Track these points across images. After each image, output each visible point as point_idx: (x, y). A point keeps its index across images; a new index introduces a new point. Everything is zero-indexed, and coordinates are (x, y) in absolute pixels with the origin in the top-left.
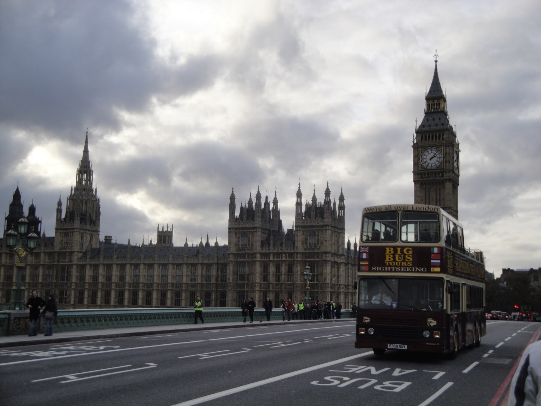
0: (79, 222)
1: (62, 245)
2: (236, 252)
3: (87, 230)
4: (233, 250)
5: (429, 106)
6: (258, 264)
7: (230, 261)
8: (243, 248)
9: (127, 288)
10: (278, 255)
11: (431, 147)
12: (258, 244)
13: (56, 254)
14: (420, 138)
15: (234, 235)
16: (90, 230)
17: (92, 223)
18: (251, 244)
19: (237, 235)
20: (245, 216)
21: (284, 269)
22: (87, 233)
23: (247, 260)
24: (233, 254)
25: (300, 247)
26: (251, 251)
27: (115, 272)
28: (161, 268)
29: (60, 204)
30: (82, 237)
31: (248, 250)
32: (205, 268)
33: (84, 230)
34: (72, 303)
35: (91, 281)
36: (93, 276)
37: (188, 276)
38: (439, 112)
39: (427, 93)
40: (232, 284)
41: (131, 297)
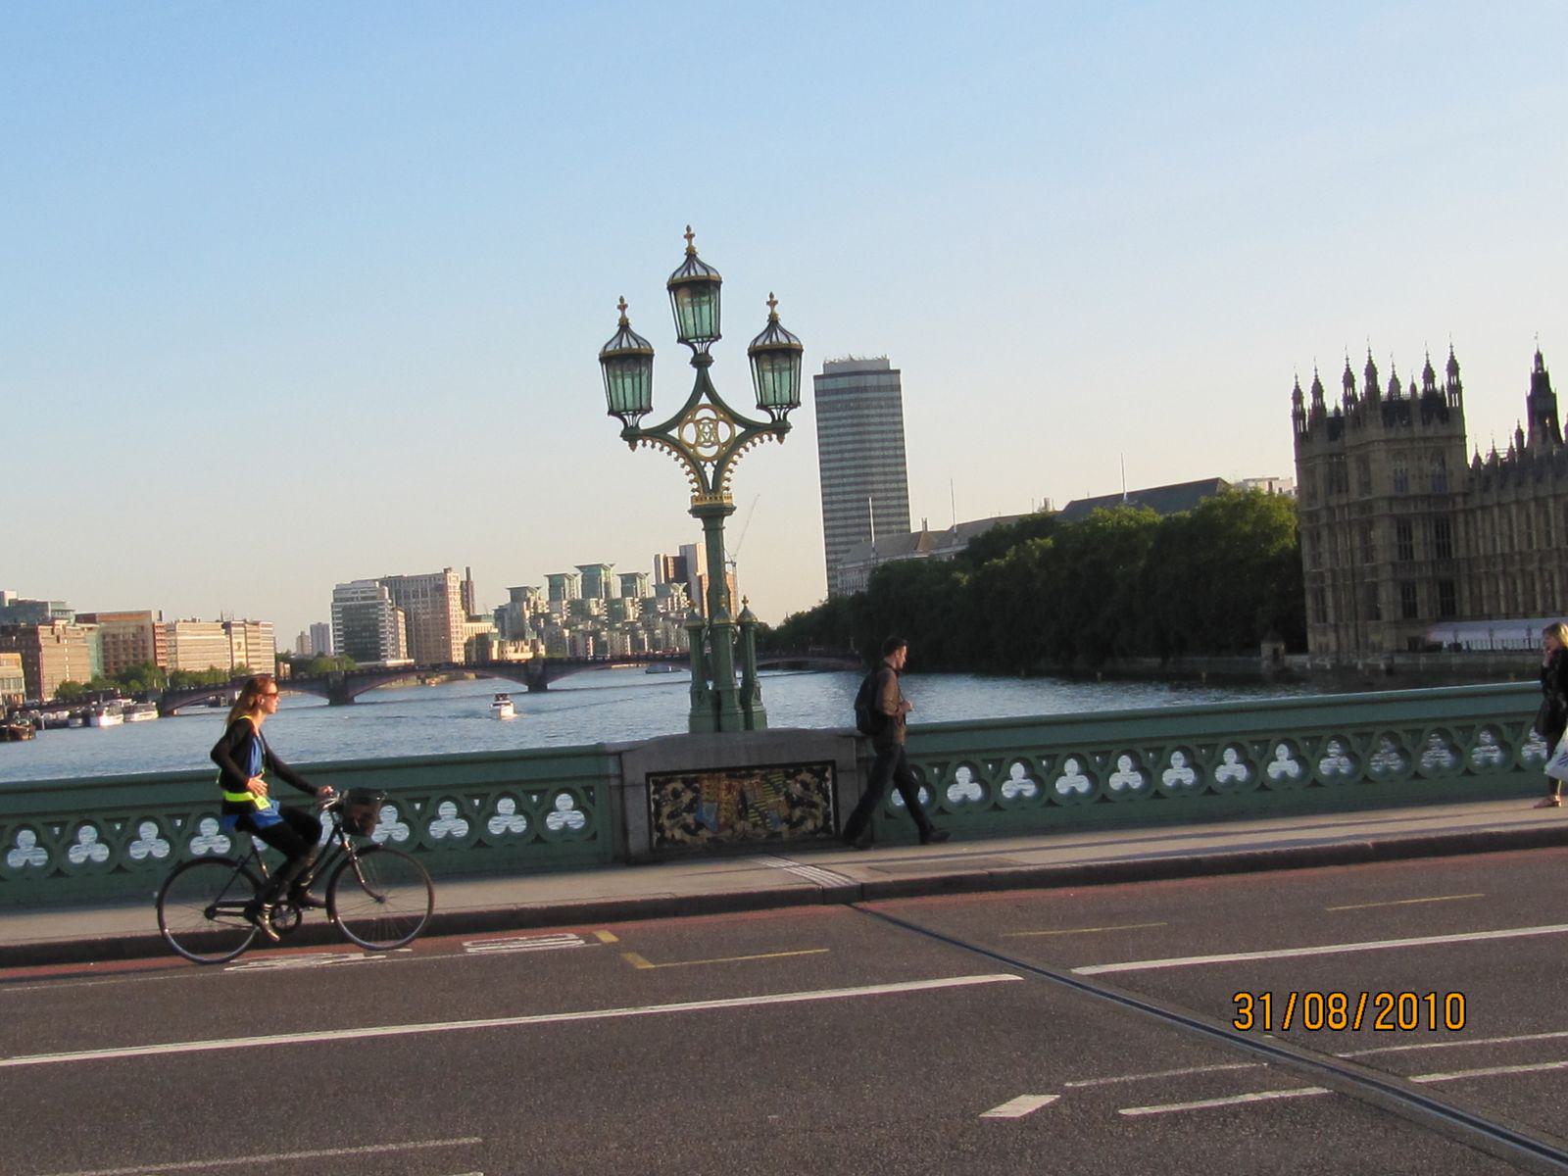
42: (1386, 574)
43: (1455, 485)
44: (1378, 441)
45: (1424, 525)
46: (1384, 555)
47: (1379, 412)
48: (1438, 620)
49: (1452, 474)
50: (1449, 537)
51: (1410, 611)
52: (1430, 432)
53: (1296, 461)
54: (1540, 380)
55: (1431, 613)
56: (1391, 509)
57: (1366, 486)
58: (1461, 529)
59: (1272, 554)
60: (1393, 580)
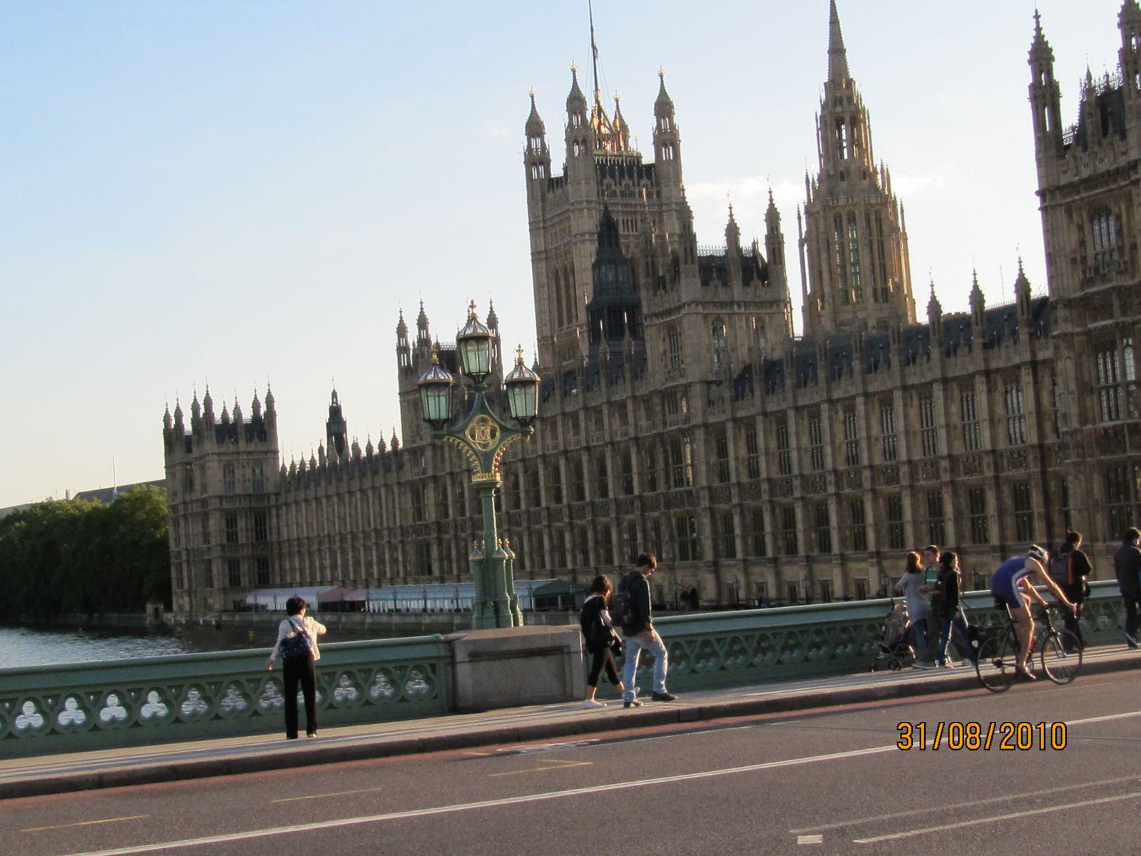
0: (699, 281)
1: (666, 366)
2: (1079, 294)
3: (732, 303)
7: (1059, 336)
8: (1097, 270)
9: (831, 489)
16: (745, 303)
17: (755, 275)
18: (1127, 250)
19: (1075, 216)
22: (734, 314)
23: (1122, 319)
24: (1069, 304)
26: (1133, 277)
27: (798, 437)
28: (916, 402)
31: (1120, 273)
33: (722, 304)
34: (709, 556)
35: (745, 479)
36: (749, 459)
37: (999, 420)
40: (1079, 437)
41: (849, 521)
42: (216, 553)
43: (269, 488)
44: (213, 454)
45: (246, 516)
46: (217, 538)
47: (214, 433)
48: (256, 587)
49: (267, 479)
50: (265, 525)
51: (234, 580)
52: (252, 448)
53: (165, 467)
54: (335, 412)
55: (250, 582)
56: (221, 505)
57: (204, 487)
58: (274, 520)
59: (158, 536)
60: (222, 557)
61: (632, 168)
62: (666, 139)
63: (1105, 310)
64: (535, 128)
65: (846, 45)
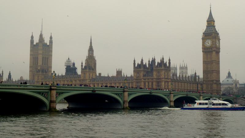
4: (135, 78)
5: (208, 24)
6: (142, 82)
10: (149, 79)
11: (208, 39)
12: (143, 75)
13: (82, 80)
14: (204, 36)
15: (135, 73)
20: (138, 67)
21: (150, 84)
24: (135, 79)
25: (155, 76)
29: (82, 63)
30: (89, 75)
32: (128, 84)
38: (211, 26)
39: (207, 18)
54: (10, 74)
61: (45, 45)
62: (51, 42)
63: (138, 80)
64: (32, 37)
65: (92, 42)
